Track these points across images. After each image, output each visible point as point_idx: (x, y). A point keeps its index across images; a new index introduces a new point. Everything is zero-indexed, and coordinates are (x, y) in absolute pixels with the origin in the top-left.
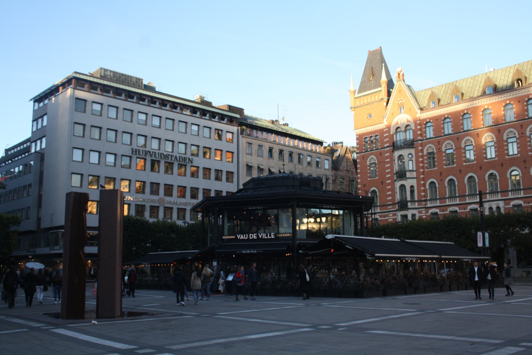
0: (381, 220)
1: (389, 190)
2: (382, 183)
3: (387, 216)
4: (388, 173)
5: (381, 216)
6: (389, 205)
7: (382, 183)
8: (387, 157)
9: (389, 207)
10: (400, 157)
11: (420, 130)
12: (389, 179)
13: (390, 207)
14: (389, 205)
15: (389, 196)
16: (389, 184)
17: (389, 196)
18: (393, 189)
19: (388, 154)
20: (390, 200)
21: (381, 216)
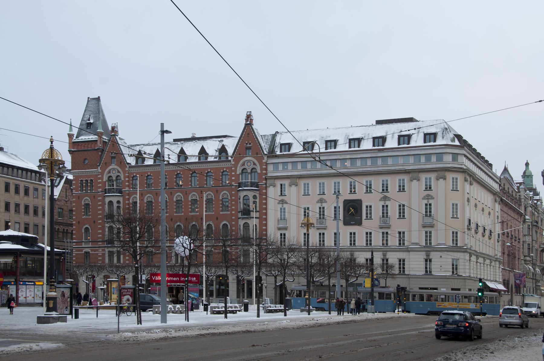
0: (92, 254)
1: (100, 229)
2: (94, 222)
3: (97, 251)
4: (100, 214)
5: (92, 251)
6: (99, 242)
7: (94, 222)
8: (99, 201)
9: (99, 243)
10: (111, 203)
11: (128, 181)
12: (100, 219)
13: (100, 243)
14: (99, 242)
15: (100, 233)
16: (100, 224)
17: (100, 233)
18: (103, 228)
19: (100, 198)
20: (100, 238)
21: (92, 251)
